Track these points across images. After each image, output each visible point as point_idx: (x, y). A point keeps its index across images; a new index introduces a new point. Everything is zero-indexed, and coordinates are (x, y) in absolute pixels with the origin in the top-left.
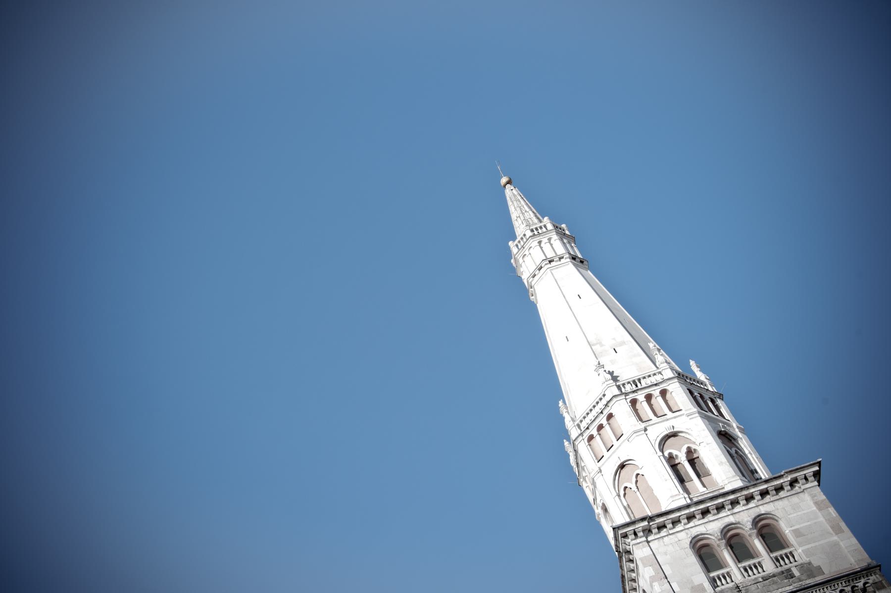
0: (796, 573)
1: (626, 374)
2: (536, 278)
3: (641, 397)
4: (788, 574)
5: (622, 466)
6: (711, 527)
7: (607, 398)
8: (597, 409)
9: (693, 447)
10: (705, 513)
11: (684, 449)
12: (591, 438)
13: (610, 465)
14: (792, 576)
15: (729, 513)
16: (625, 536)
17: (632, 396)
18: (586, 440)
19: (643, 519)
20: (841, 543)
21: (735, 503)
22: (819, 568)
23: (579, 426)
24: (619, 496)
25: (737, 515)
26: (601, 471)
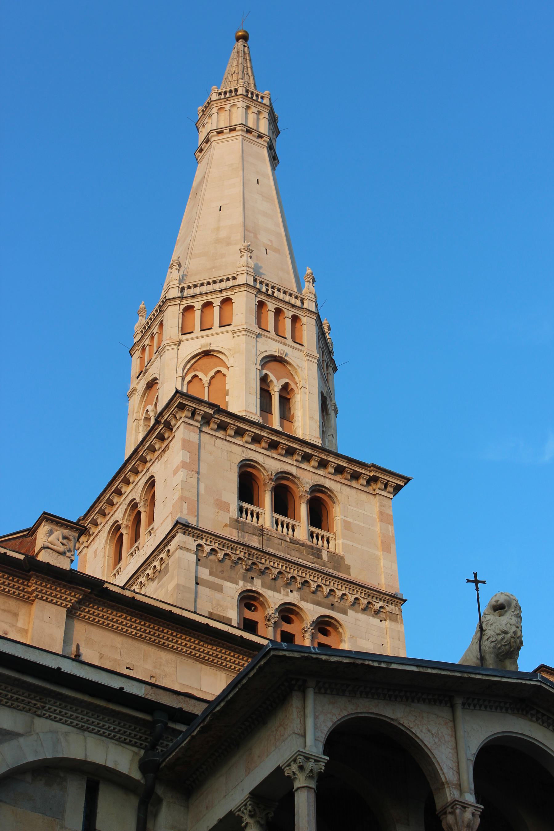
0: (325, 557)
1: (271, 276)
2: (221, 136)
3: (271, 306)
4: (317, 553)
5: (207, 354)
6: (271, 464)
7: (237, 282)
8: (217, 287)
9: (292, 385)
10: (273, 445)
11: (283, 381)
12: (189, 308)
13: (193, 345)
14: (320, 557)
15: (295, 463)
16: (181, 407)
17: (262, 298)
18: (182, 307)
19: (211, 405)
20: (382, 562)
21: (307, 458)
22: (348, 567)
23: (183, 289)
24: (183, 379)
25: (301, 471)
26: (179, 344)
